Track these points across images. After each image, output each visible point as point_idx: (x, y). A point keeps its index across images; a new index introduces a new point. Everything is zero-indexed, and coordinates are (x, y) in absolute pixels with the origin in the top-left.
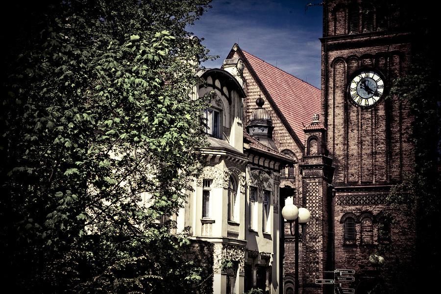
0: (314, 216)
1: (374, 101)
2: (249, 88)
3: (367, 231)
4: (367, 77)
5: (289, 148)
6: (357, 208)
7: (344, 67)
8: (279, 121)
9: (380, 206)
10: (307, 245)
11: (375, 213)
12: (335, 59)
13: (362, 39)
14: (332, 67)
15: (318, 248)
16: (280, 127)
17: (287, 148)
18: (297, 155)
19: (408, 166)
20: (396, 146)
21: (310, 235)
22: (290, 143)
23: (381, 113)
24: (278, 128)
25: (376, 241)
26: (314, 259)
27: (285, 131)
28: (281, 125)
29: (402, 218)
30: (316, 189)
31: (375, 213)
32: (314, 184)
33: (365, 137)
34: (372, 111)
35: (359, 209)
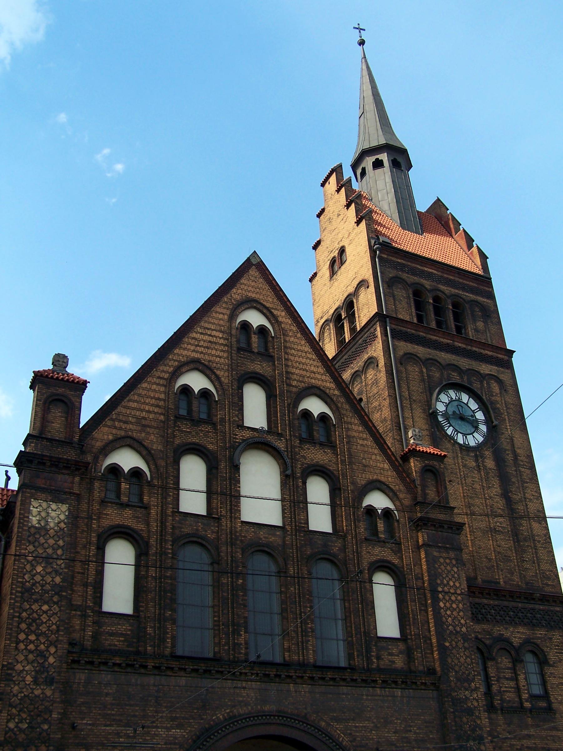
0: (458, 629)
1: (477, 442)
2: (287, 339)
3: (507, 679)
4: (459, 400)
5: (383, 479)
6: (484, 630)
7: (421, 372)
8: (356, 421)
9: (521, 629)
10: (454, 694)
11: (516, 641)
12: (405, 354)
13: (442, 340)
14: (401, 364)
15: (476, 704)
16: (360, 432)
17: (379, 478)
18: (401, 496)
19: (547, 563)
20: (521, 524)
21: (456, 672)
22: (383, 469)
23: (490, 463)
24: (356, 434)
25: (527, 701)
26: (473, 730)
27: (370, 442)
28: (360, 429)
29: (557, 656)
30: (453, 573)
31: (516, 641)
32: (448, 561)
33: (471, 497)
34: (476, 456)
35: (489, 633)
